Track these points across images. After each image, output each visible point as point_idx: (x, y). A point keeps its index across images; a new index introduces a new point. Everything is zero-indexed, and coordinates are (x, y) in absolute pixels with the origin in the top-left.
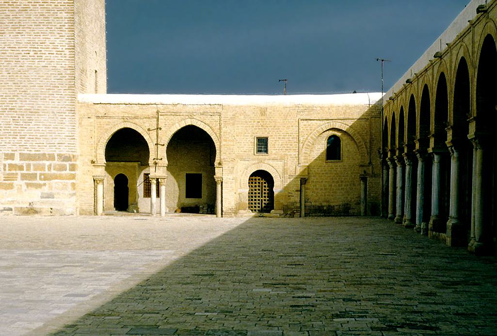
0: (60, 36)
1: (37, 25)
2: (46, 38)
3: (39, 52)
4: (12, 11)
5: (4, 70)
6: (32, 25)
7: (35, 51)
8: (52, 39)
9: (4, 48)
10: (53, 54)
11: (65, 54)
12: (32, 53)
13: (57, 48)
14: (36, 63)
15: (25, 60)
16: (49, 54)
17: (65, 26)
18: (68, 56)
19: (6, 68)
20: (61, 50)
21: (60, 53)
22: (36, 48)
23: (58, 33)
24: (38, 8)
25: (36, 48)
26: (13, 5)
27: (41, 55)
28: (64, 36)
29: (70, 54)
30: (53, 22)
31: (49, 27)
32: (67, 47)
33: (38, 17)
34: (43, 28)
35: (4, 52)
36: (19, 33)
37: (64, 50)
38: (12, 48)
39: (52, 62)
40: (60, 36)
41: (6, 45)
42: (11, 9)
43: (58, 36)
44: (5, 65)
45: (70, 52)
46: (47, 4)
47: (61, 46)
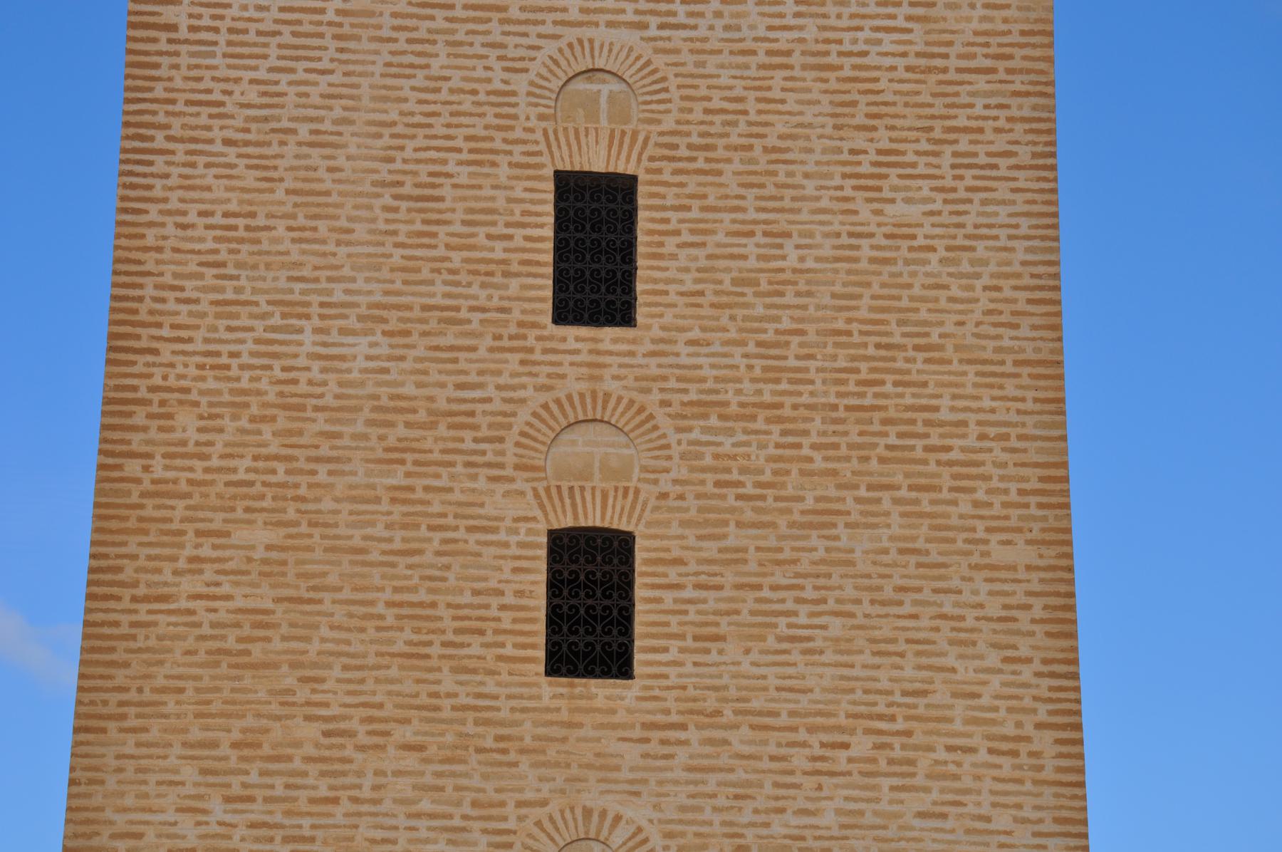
0: (1006, 660)
1: (883, 603)
2: (930, 668)
3: (896, 741)
4: (754, 525)
5: (717, 829)
6: (858, 602)
7: (880, 732)
8: (965, 671)
9: (718, 713)
10: (972, 750)
11: (1032, 754)
12: (861, 745)
13: (993, 722)
14: (886, 794)
15: (825, 780)
16: (950, 749)
17: (1028, 607)
18: (1049, 764)
19: (727, 817)
20: (1009, 730)
21: (1006, 747)
22: (880, 717)
23: (995, 646)
24: (887, 514)
25: (880, 717)
26: (762, 498)
27: (911, 754)
28: (1029, 660)
29: (1061, 755)
30: (966, 587)
31: (948, 609)
32: (1042, 716)
33: (885, 559)
34: (914, 617)
35: (718, 734)
36: (792, 639)
37: (1029, 730)
38: (760, 714)
39: (967, 792)
40: (1006, 660)
41: (726, 700)
42: (749, 516)
43: (993, 659)
44: (721, 801)
45: (1059, 742)
46: (934, 495)
47: (1010, 710)
